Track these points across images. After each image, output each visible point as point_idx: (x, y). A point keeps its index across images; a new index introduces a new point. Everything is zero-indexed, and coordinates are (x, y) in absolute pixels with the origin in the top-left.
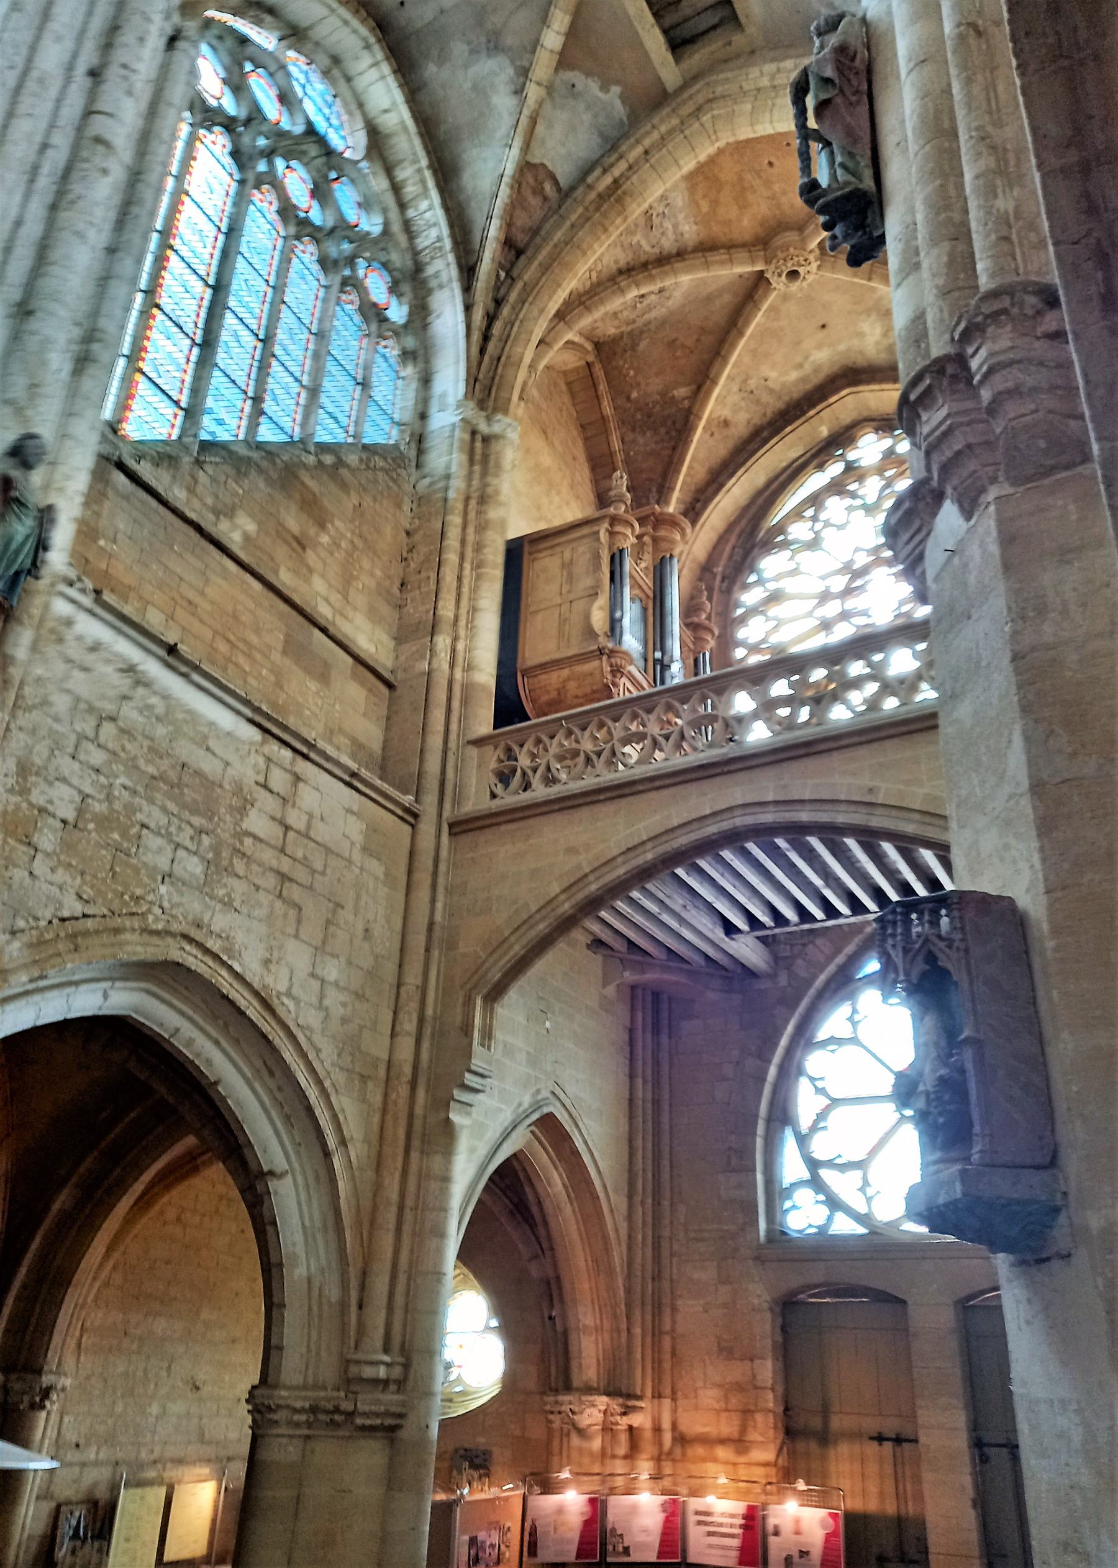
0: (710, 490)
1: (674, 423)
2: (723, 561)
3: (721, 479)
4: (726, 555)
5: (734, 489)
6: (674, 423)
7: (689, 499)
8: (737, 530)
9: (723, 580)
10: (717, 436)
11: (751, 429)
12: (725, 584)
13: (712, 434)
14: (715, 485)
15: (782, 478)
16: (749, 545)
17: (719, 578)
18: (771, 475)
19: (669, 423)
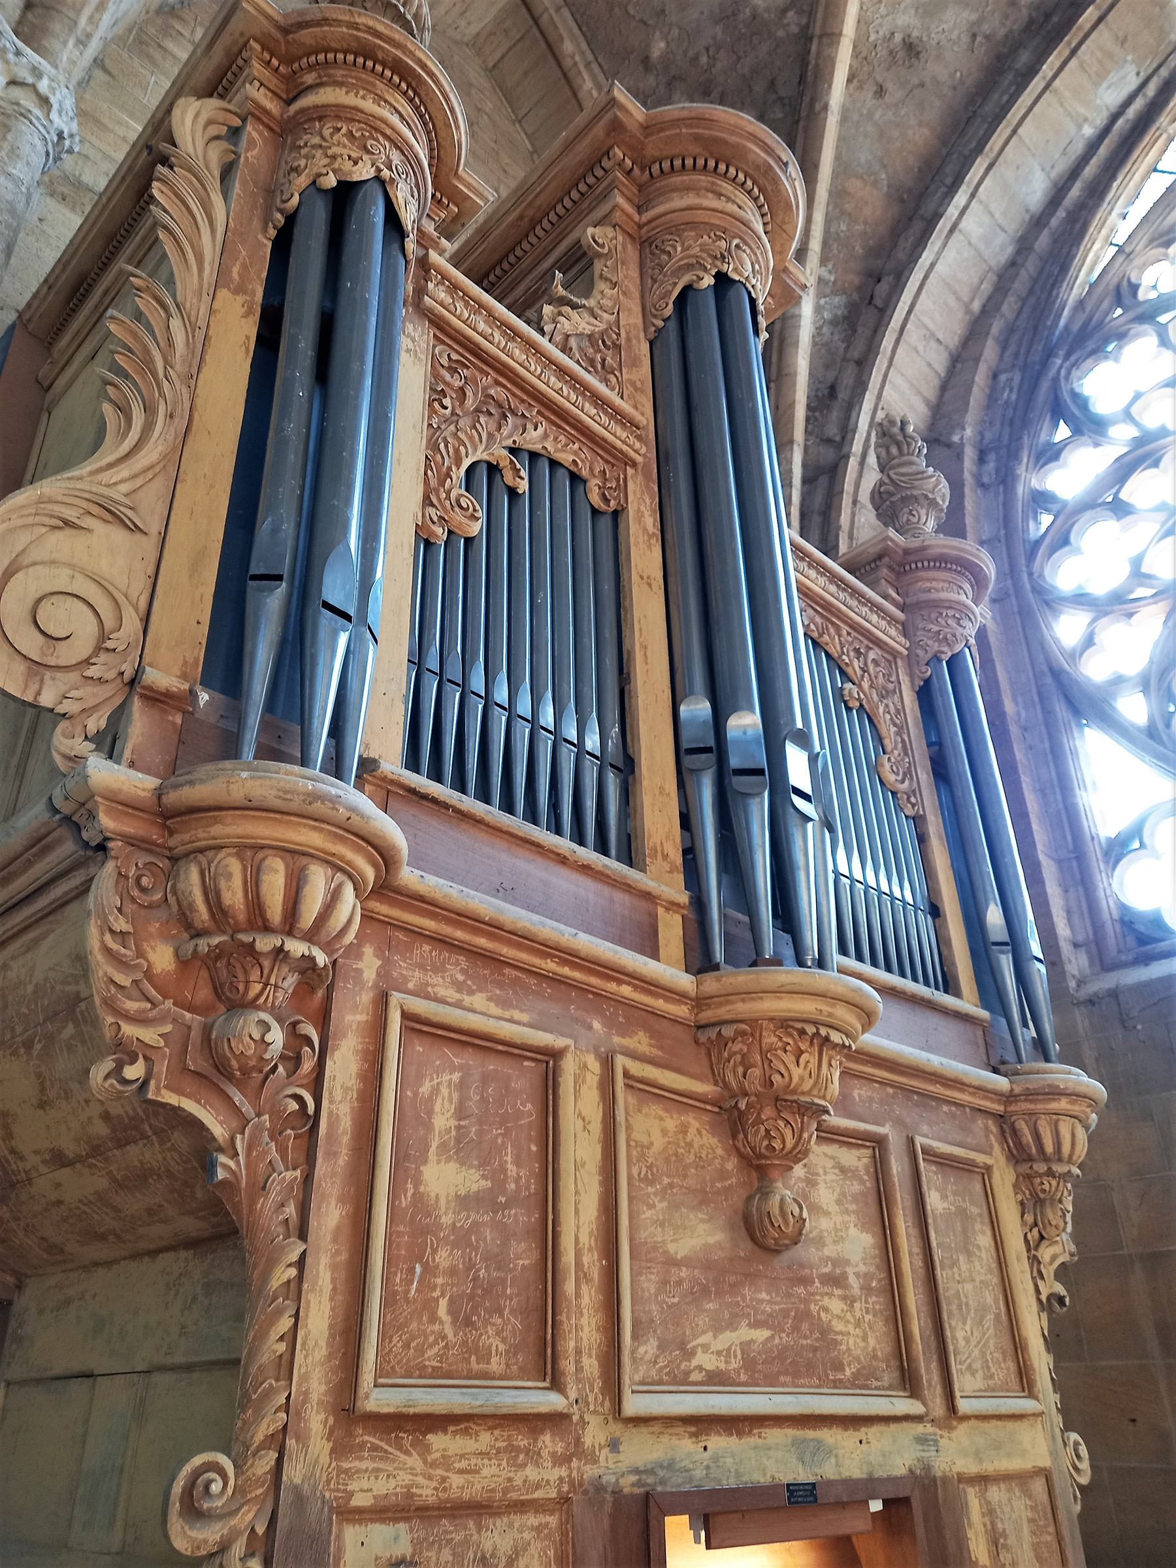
0: (906, 243)
1: (772, 84)
2: (972, 416)
3: (928, 208)
4: (977, 396)
5: (967, 224)
6: (772, 84)
7: (854, 279)
8: (997, 327)
9: (981, 459)
10: (894, 93)
11: (982, 50)
12: (991, 466)
13: (880, 91)
14: (917, 226)
15: (1089, 171)
16: (1036, 356)
17: (969, 454)
18: (1063, 166)
19: (759, 88)
